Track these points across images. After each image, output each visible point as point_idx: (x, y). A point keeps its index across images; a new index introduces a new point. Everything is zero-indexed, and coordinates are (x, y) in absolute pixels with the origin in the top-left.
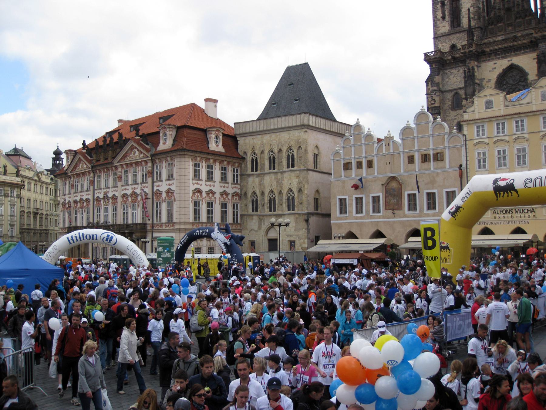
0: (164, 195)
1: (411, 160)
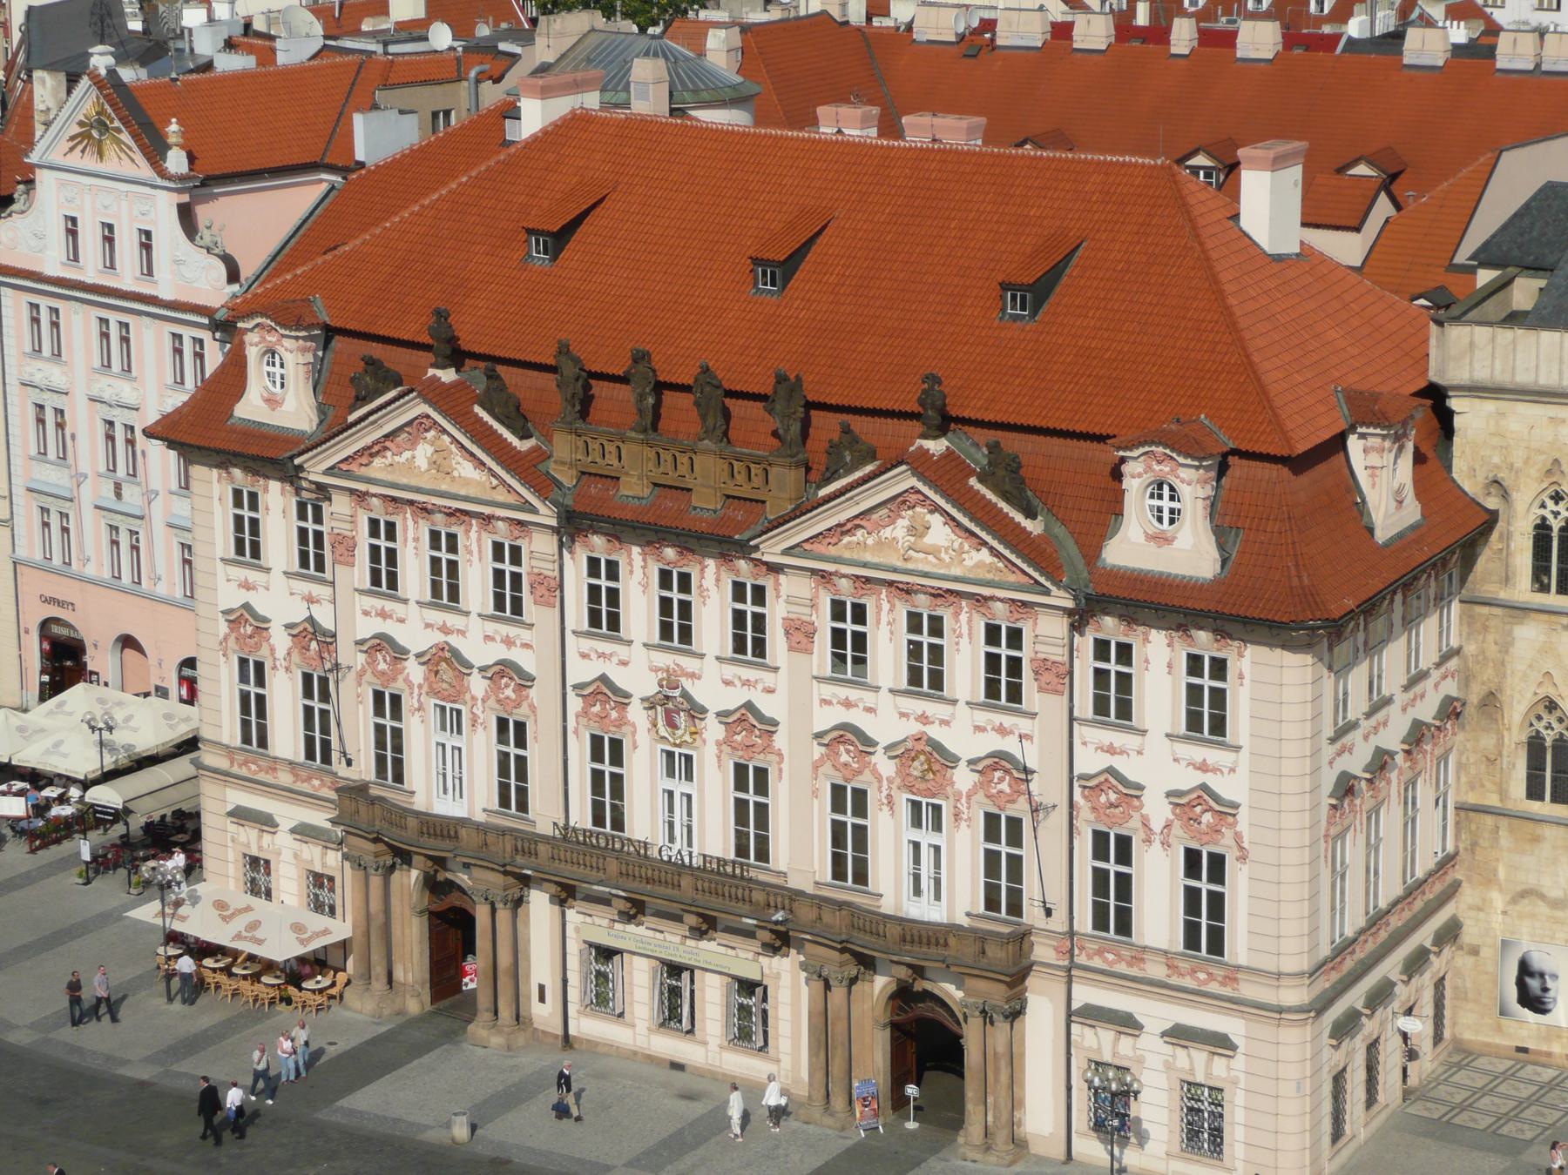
0: (1157, 809)
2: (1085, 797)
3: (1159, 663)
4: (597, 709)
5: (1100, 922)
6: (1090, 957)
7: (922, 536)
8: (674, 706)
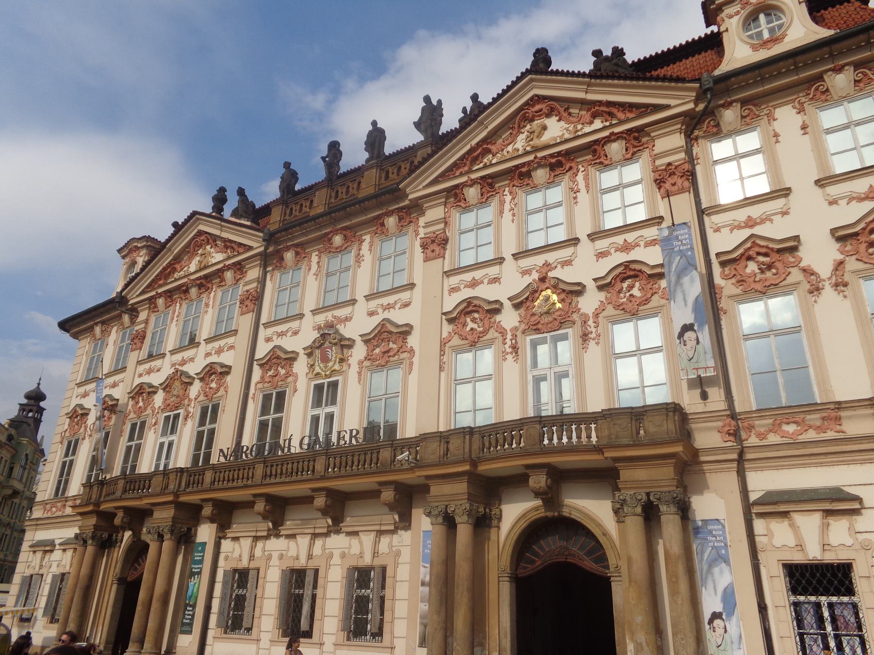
0: (820, 254)
2: (725, 277)
4: (270, 373)
6: (762, 436)
7: (539, 136)
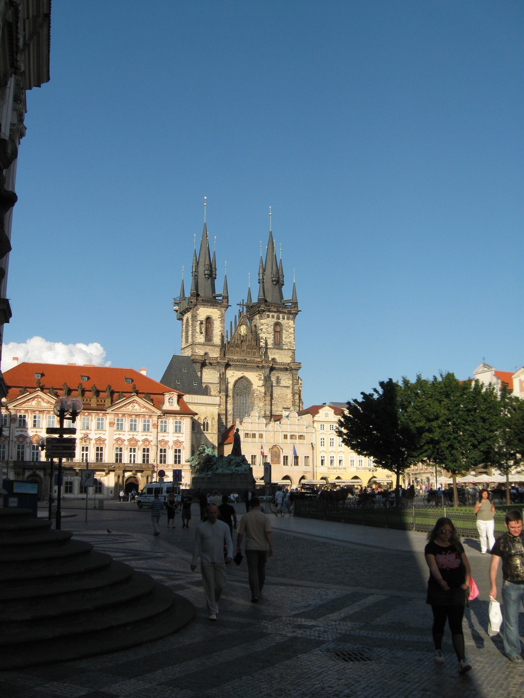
0: (171, 444)
1: (285, 437)
3: (171, 422)
5: (161, 462)
8: (86, 438)
